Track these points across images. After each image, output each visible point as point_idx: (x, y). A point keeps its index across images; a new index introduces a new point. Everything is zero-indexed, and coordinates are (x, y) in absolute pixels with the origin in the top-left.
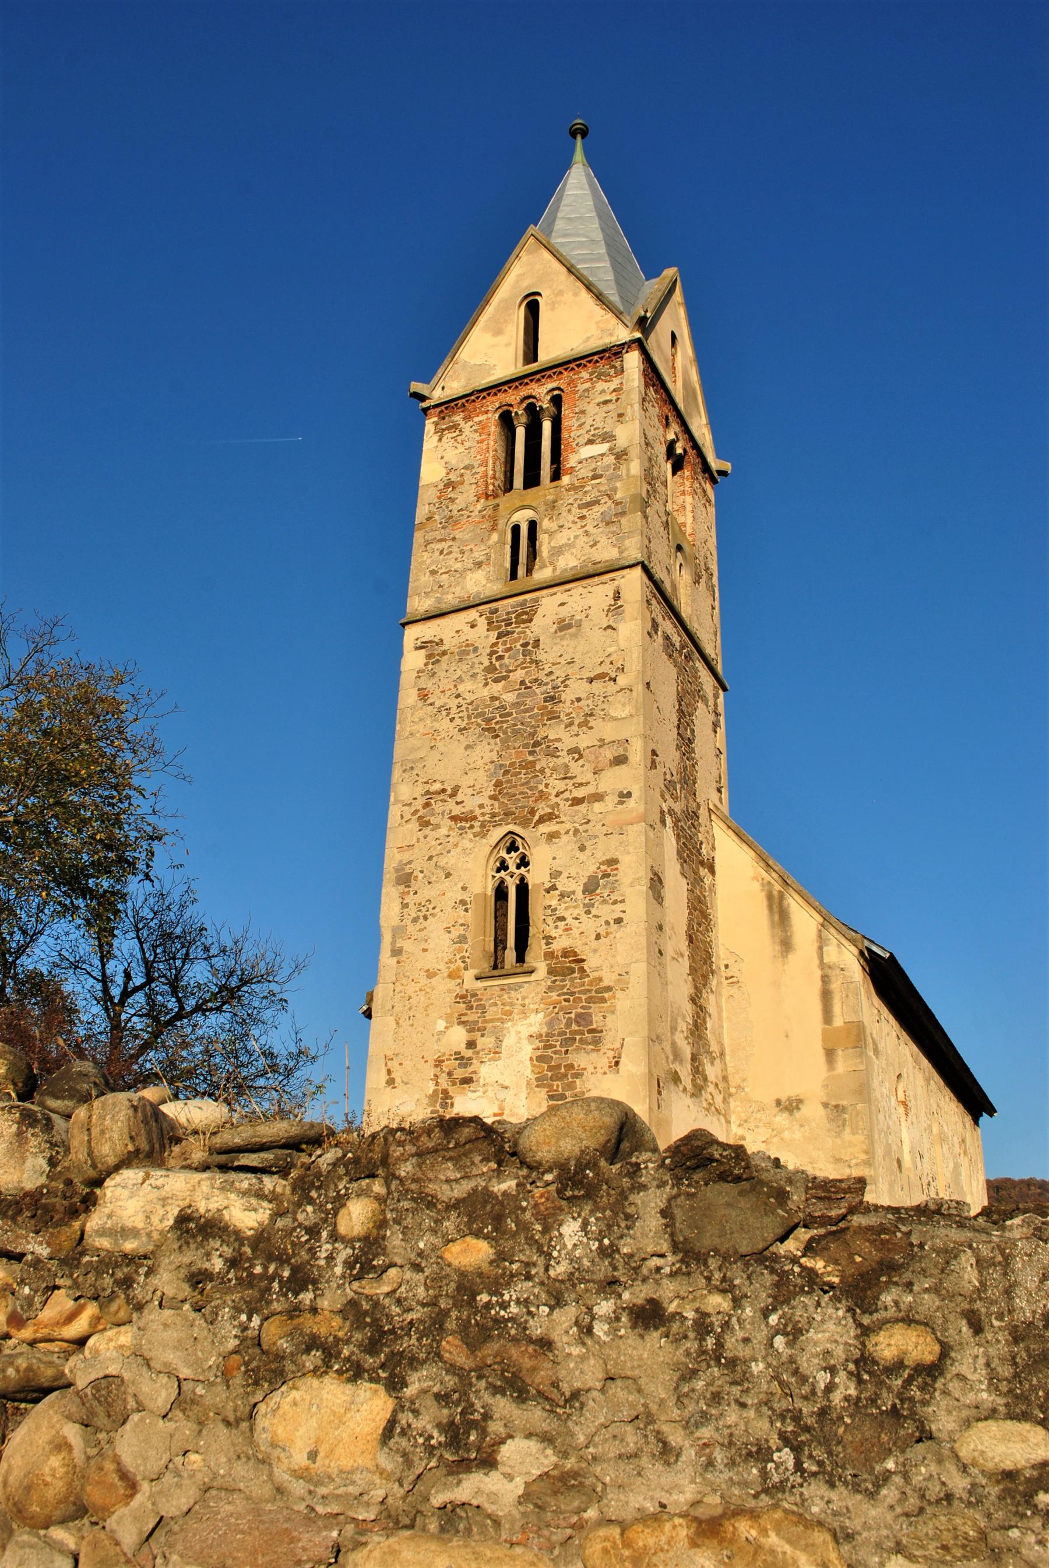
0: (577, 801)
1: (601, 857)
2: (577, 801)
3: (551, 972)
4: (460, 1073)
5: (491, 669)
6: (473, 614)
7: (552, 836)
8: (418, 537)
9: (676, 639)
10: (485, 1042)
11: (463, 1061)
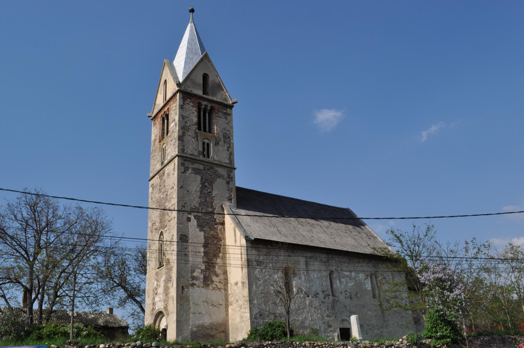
0: (169, 221)
1: (172, 234)
2: (169, 221)
3: (166, 265)
4: (156, 292)
5: (160, 189)
6: (157, 175)
7: (166, 231)
8: (151, 156)
9: (201, 167)
10: (159, 284)
11: (156, 289)
